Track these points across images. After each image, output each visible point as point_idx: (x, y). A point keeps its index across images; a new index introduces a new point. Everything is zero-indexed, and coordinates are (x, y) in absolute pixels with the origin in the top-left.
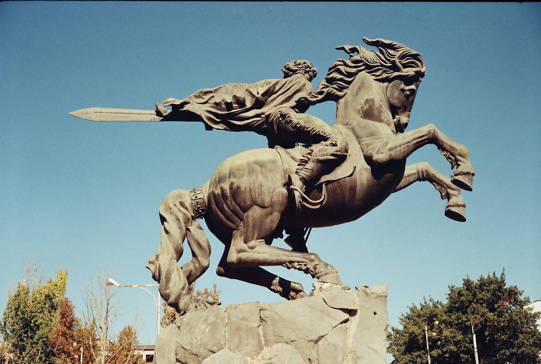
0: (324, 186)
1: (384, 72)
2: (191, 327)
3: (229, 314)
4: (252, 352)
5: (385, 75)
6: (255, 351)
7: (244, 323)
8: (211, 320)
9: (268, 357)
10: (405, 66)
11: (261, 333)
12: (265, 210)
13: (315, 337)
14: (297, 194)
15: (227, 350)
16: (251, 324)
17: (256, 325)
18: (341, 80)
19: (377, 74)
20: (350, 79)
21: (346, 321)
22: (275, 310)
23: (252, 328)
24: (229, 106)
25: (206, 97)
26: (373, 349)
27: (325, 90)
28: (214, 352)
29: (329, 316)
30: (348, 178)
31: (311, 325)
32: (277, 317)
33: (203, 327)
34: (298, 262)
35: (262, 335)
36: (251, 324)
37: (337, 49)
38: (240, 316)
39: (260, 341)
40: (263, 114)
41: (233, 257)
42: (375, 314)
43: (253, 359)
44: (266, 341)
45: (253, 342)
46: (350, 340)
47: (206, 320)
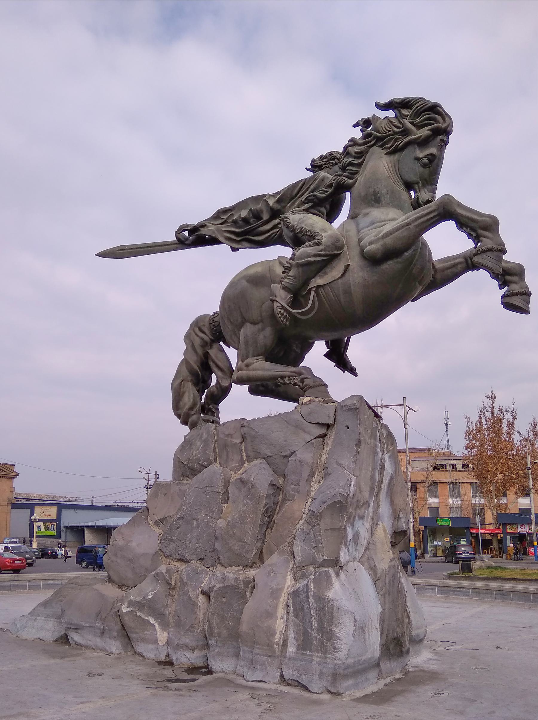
2: (192, 444)
3: (218, 431)
4: (235, 466)
6: (238, 466)
7: (229, 439)
8: (205, 436)
11: (243, 448)
12: (257, 326)
13: (288, 453)
15: (218, 465)
16: (234, 440)
17: (238, 441)
21: (323, 436)
22: (252, 426)
23: (236, 443)
26: (340, 465)
29: (304, 431)
30: (340, 281)
31: (285, 441)
32: (253, 433)
33: (199, 443)
34: (289, 377)
35: (243, 451)
36: (234, 440)
38: (227, 433)
42: (348, 428)
43: (235, 473)
44: (248, 457)
45: (237, 457)
46: (324, 457)
47: (201, 437)
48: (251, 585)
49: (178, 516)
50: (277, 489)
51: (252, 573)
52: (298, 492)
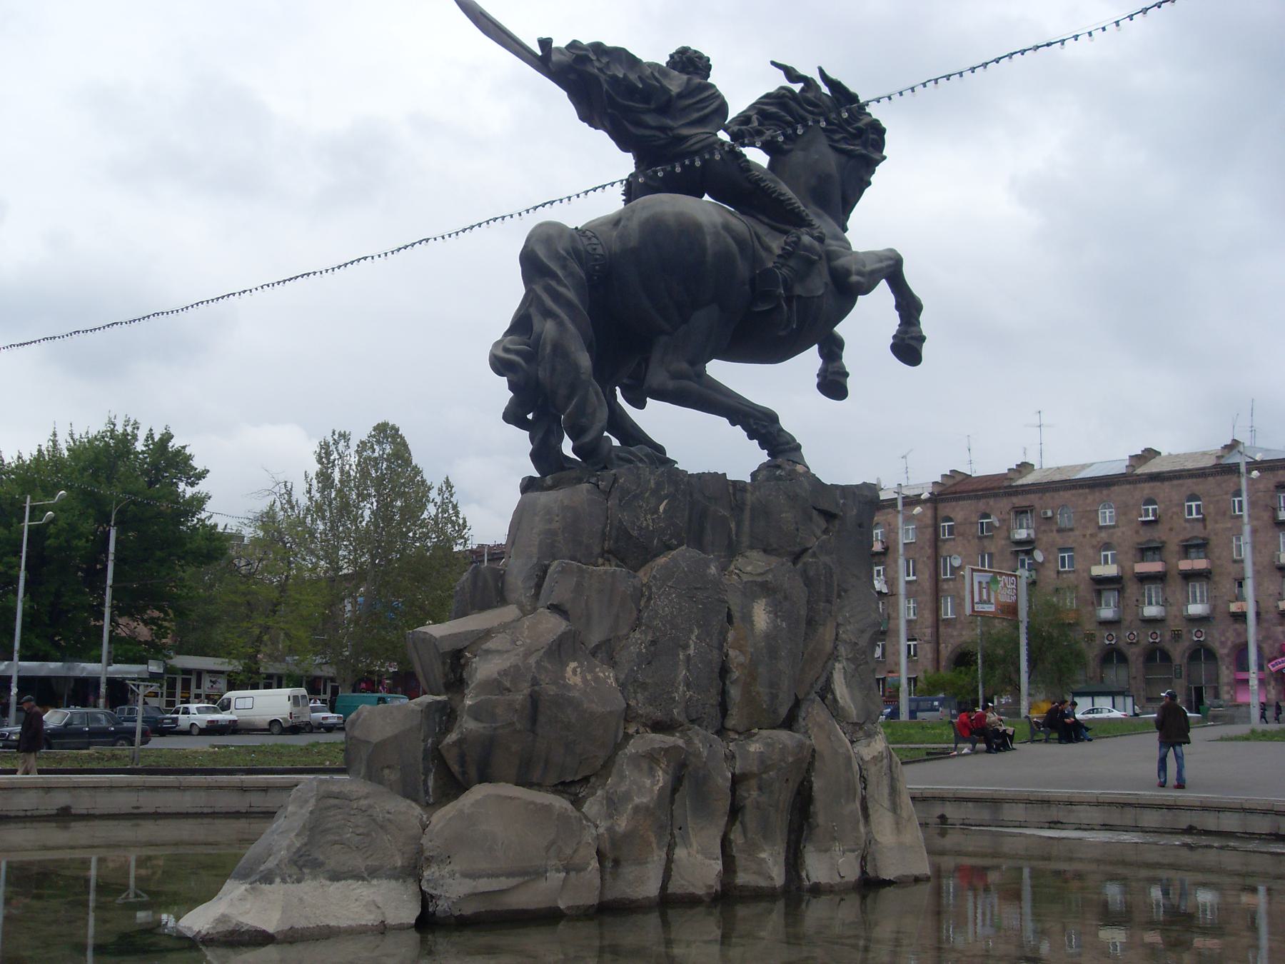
13: (797, 549)
19: (837, 137)
37: (773, 63)
40: (671, 129)
49: (649, 638)
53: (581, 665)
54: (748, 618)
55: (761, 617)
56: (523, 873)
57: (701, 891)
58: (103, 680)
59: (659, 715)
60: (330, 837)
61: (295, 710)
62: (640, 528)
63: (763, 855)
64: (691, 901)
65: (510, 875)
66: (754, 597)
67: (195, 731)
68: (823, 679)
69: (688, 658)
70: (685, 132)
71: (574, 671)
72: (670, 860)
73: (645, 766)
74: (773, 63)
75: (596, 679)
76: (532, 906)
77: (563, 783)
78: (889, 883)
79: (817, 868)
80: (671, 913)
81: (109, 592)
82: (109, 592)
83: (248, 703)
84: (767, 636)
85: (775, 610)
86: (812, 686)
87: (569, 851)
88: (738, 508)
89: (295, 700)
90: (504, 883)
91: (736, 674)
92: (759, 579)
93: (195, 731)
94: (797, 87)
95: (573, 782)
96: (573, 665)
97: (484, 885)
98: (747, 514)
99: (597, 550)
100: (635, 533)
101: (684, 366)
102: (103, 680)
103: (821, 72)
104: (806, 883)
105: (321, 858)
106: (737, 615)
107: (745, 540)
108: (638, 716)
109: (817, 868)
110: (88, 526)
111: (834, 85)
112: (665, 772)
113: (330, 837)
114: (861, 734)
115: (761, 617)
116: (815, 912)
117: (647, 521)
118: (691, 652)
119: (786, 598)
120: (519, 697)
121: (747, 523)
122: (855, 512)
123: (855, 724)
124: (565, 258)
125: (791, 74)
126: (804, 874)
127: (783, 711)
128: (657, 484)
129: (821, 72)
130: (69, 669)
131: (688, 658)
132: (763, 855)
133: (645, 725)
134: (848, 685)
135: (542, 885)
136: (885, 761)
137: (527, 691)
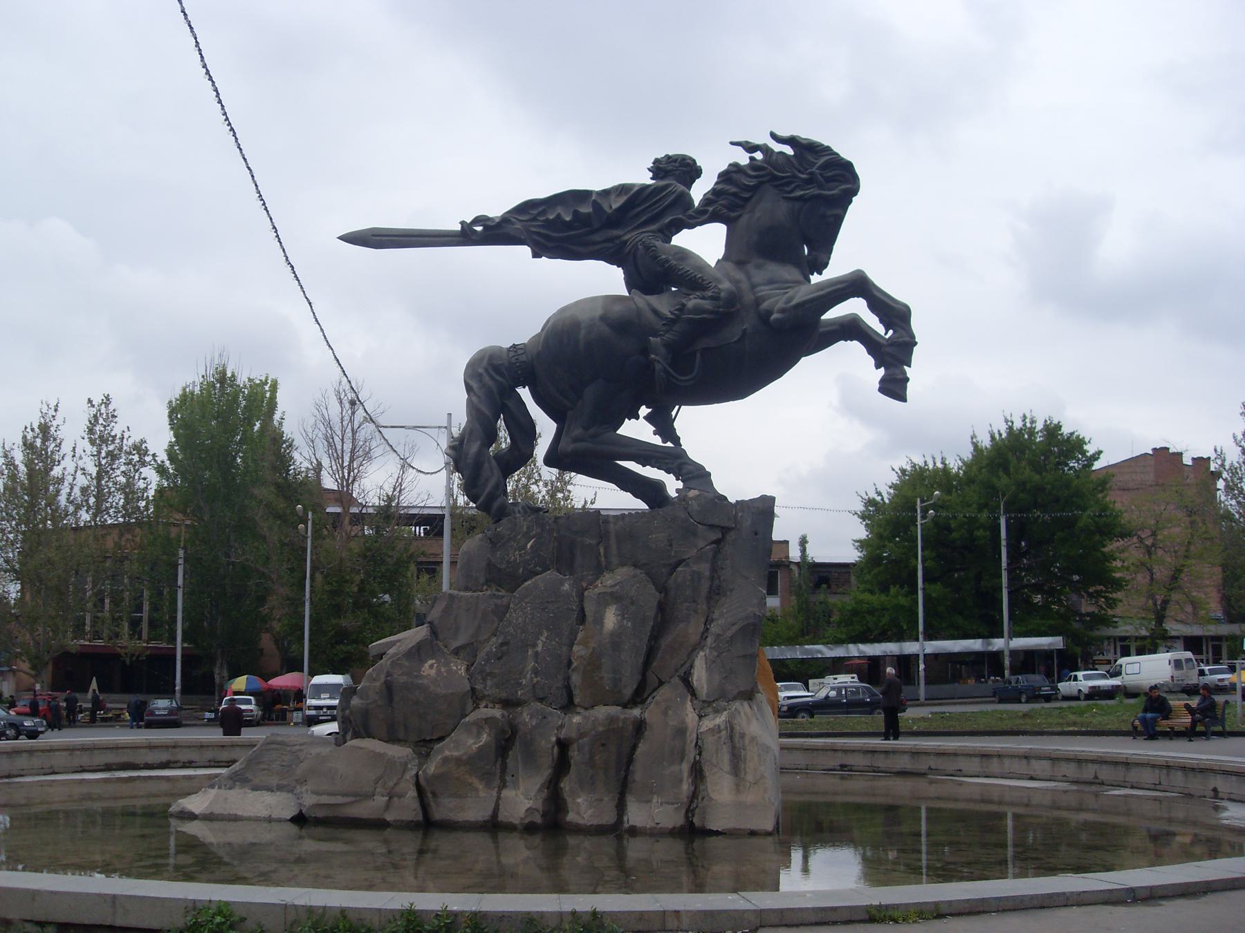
0: (698, 355)
1: (797, 187)
5: (799, 193)
9: (609, 582)
10: (828, 180)
11: (602, 550)
13: (673, 561)
14: (658, 367)
17: (594, 542)
18: (734, 195)
19: (788, 189)
20: (746, 195)
21: (717, 542)
24: (568, 226)
25: (535, 212)
27: (711, 209)
28: (537, 574)
37: (732, 143)
39: (599, 562)
40: (619, 237)
41: (566, 446)
48: (640, 727)
50: (662, 608)
51: (636, 712)
52: (696, 611)
53: (438, 662)
54: (599, 621)
55: (611, 619)
56: (356, 795)
57: (516, 822)
58: (1007, 653)
59: (504, 695)
60: (263, 766)
61: (1177, 673)
62: (508, 562)
63: (579, 800)
64: (510, 828)
65: (344, 795)
66: (607, 604)
67: (1082, 697)
68: (687, 665)
69: (536, 654)
70: (626, 237)
71: (431, 666)
72: (499, 798)
73: (475, 730)
74: (732, 143)
75: (449, 671)
76: (365, 816)
77: (424, 740)
78: (717, 833)
79: (636, 815)
80: (501, 835)
81: (1004, 574)
82: (1004, 574)
83: (1136, 668)
84: (612, 634)
85: (622, 615)
86: (677, 671)
87: (391, 784)
88: (603, 536)
89: (1178, 664)
90: (340, 800)
91: (575, 664)
92: (609, 590)
93: (1082, 697)
94: (759, 156)
95: (431, 741)
96: (430, 662)
97: (325, 799)
98: (613, 541)
99: (482, 580)
100: (503, 566)
101: (578, 432)
102: (1007, 653)
103: (773, 136)
104: (626, 825)
105: (250, 777)
106: (589, 618)
107: (615, 560)
108: (484, 697)
109: (636, 815)
110: (984, 516)
111: (791, 141)
112: (489, 735)
113: (263, 766)
114: (710, 709)
115: (611, 619)
116: (636, 849)
117: (515, 556)
118: (539, 649)
119: (632, 603)
120: (378, 684)
121: (614, 547)
122: (749, 523)
123: (704, 702)
124: (480, 375)
125: (750, 148)
126: (625, 819)
127: (628, 692)
128: (528, 528)
129: (773, 136)
130: (989, 644)
131: (536, 654)
132: (579, 800)
133: (493, 702)
134: (709, 669)
135: (371, 803)
136: (724, 733)
137: (382, 680)
